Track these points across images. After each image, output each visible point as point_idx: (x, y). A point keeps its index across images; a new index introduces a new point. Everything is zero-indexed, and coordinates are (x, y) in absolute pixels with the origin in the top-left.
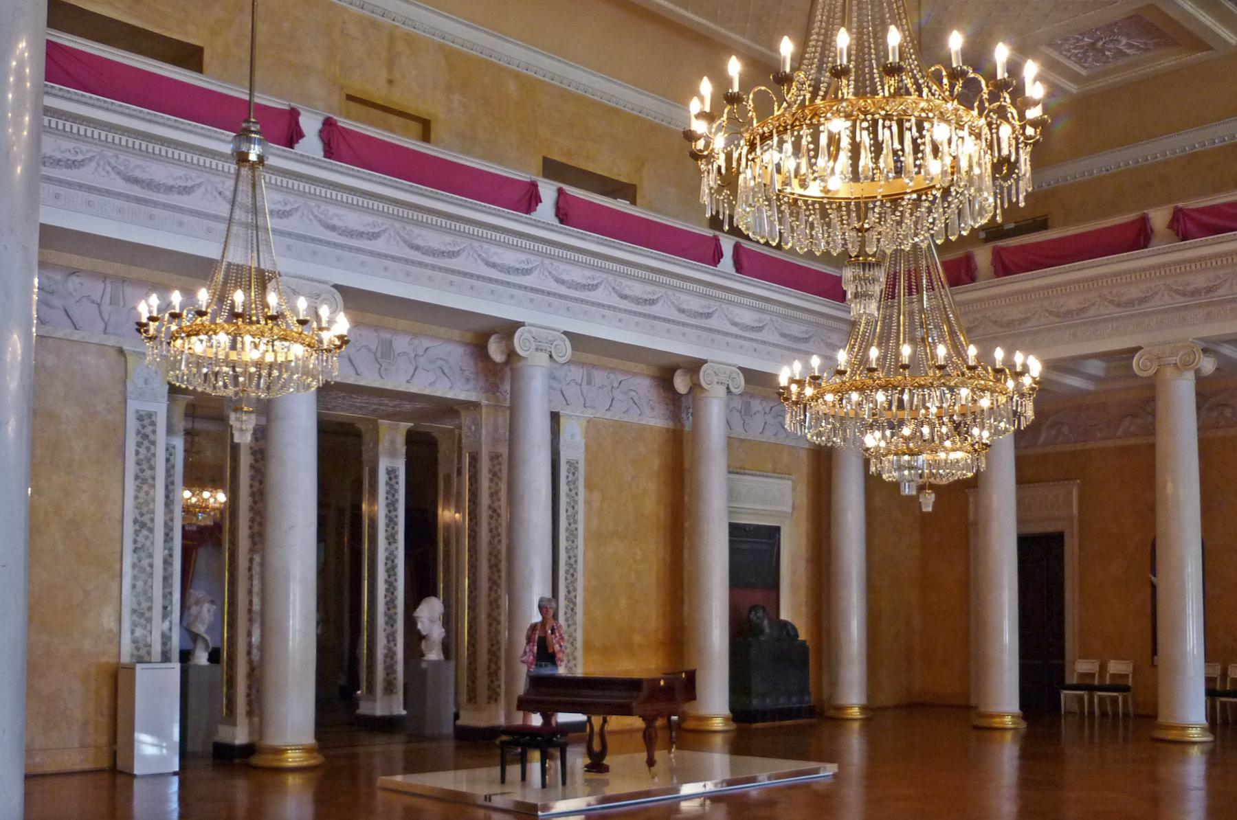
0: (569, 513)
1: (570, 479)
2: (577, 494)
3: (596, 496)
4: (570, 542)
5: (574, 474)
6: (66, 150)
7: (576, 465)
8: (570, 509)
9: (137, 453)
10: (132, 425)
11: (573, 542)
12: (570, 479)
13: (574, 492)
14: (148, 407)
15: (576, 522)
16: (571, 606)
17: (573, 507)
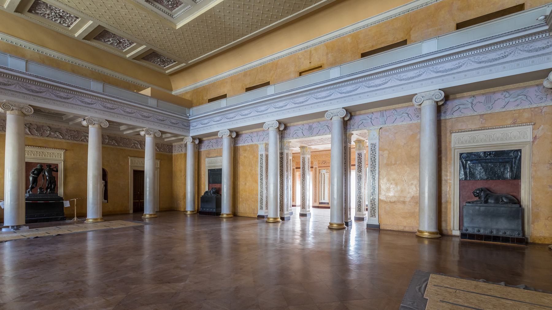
0: (372, 160)
1: (372, 149)
2: (376, 153)
3: (386, 153)
4: (373, 169)
5: (374, 147)
6: (455, 65)
7: (375, 144)
8: (373, 159)
9: (260, 162)
10: (259, 157)
11: (374, 168)
12: (372, 149)
13: (374, 153)
14: (261, 153)
15: (375, 162)
16: (374, 188)
17: (374, 158)
